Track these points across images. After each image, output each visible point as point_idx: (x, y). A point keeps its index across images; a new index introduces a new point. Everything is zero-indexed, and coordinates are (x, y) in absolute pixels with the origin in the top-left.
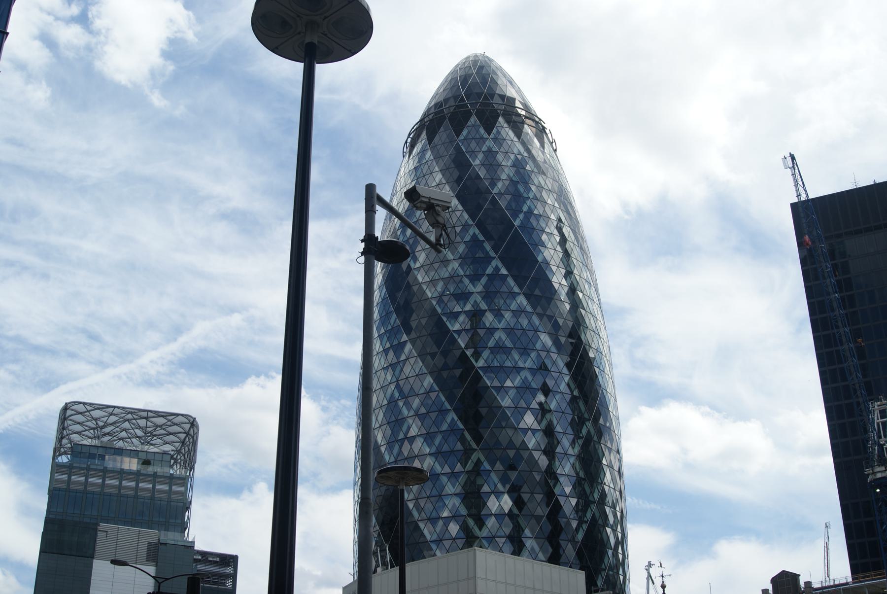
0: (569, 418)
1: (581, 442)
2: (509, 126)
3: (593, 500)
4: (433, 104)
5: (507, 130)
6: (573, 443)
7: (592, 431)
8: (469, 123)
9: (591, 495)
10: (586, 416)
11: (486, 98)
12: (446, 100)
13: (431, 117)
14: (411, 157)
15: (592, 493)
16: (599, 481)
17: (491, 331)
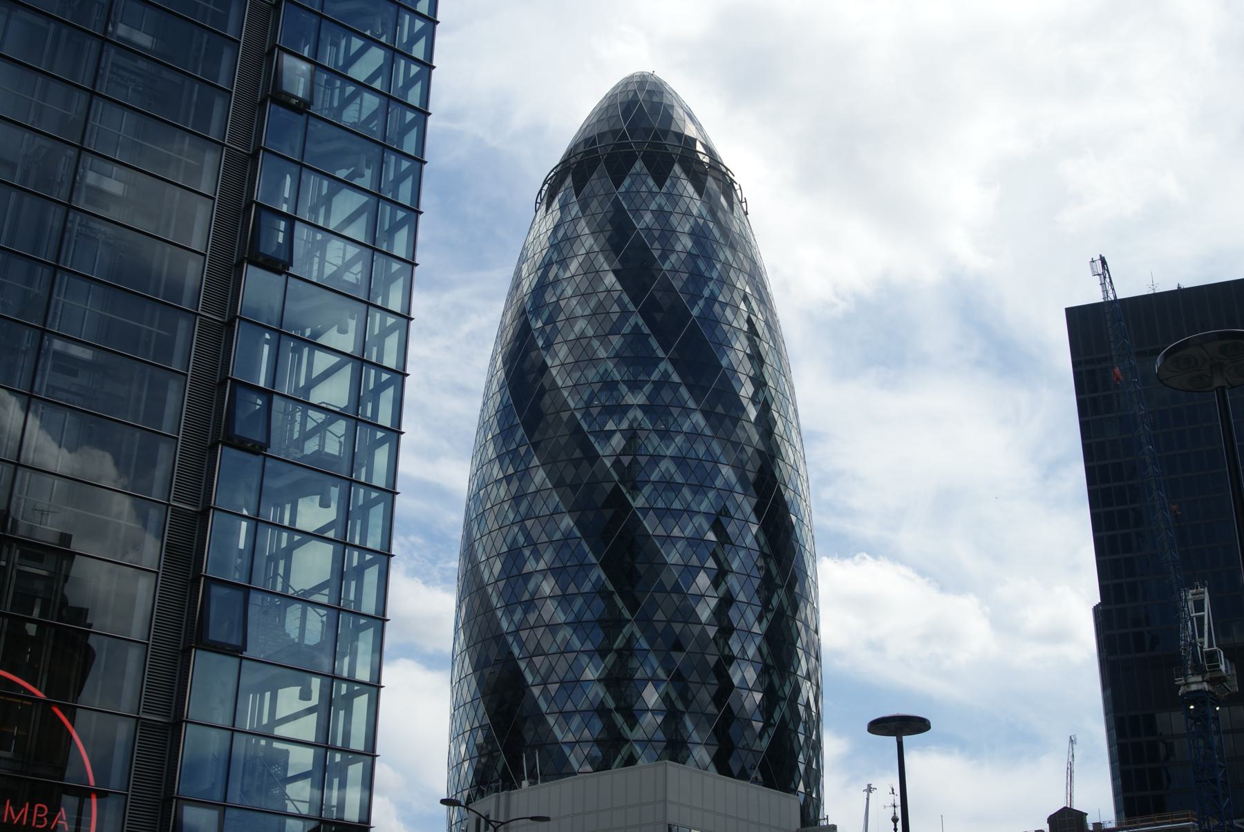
0: (757, 583)
1: (770, 616)
2: (688, 177)
3: (783, 696)
4: (582, 139)
5: (685, 182)
6: (760, 619)
7: (785, 603)
8: (633, 171)
9: (781, 688)
10: (778, 581)
11: (656, 136)
12: (601, 136)
13: (579, 157)
14: (550, 211)
15: (782, 686)
16: (792, 670)
17: (656, 459)
